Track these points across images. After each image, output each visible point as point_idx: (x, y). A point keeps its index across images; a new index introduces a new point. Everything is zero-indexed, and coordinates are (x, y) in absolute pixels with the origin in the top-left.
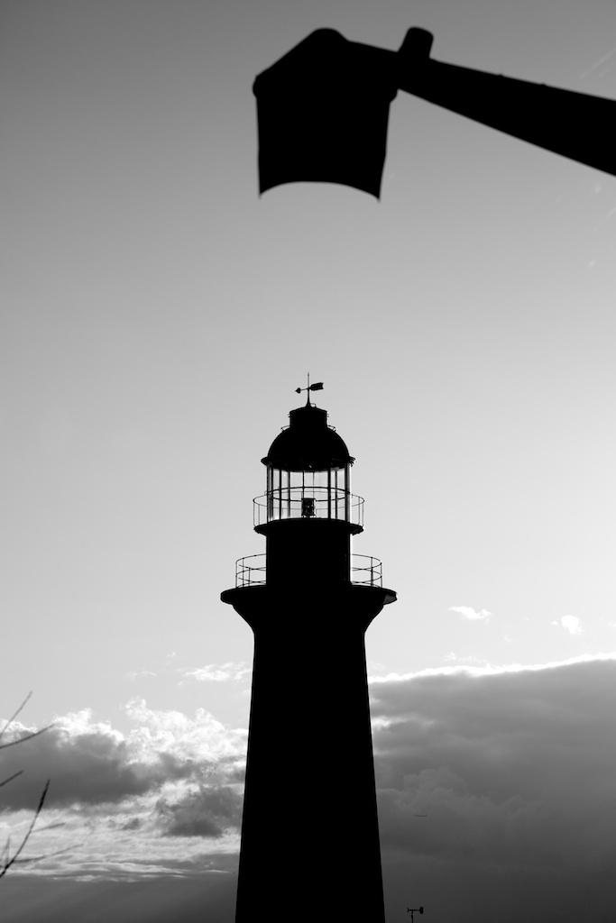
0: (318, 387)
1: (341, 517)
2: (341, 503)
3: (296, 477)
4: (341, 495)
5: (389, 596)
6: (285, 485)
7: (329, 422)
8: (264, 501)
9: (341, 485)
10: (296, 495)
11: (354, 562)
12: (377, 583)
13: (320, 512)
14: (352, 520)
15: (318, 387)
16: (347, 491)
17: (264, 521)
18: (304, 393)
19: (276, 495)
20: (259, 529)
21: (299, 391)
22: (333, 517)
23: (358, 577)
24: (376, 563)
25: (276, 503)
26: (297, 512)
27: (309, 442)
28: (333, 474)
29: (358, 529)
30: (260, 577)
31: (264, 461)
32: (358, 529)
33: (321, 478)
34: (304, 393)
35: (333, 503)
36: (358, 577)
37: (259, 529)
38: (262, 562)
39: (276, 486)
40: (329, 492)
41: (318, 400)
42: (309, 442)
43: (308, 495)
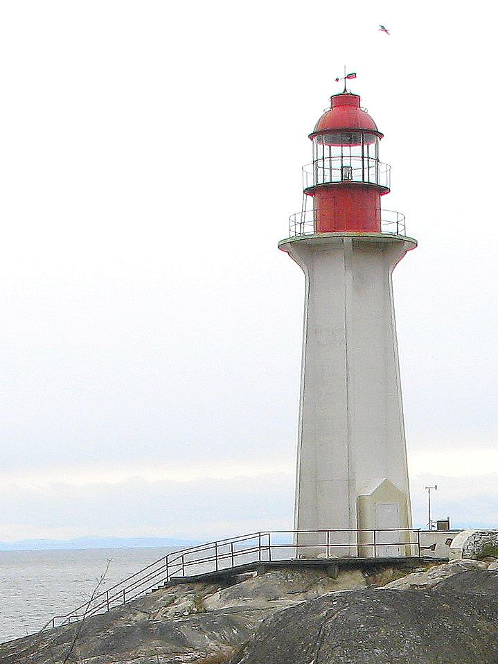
0: (352, 76)
1: (373, 180)
2: (373, 171)
3: (336, 150)
4: (372, 163)
5: (414, 244)
6: (327, 155)
7: (362, 104)
8: (310, 168)
9: (372, 155)
10: (336, 164)
11: (384, 216)
12: (402, 233)
13: (357, 177)
14: (382, 183)
15: (352, 76)
16: (377, 160)
17: (311, 184)
18: (342, 82)
19: (320, 164)
20: (309, 191)
21: (337, 80)
22: (366, 180)
23: (387, 228)
24: (401, 218)
25: (320, 171)
26: (337, 178)
27: (346, 124)
28: (365, 147)
29: (384, 190)
30: (309, 229)
31: (311, 136)
32: (384, 190)
33: (356, 150)
34: (342, 82)
35: (366, 171)
36: (387, 228)
37: (309, 191)
38: (310, 217)
39: (320, 156)
40: (363, 160)
41: (353, 87)
42: (346, 124)
43: (346, 163)
